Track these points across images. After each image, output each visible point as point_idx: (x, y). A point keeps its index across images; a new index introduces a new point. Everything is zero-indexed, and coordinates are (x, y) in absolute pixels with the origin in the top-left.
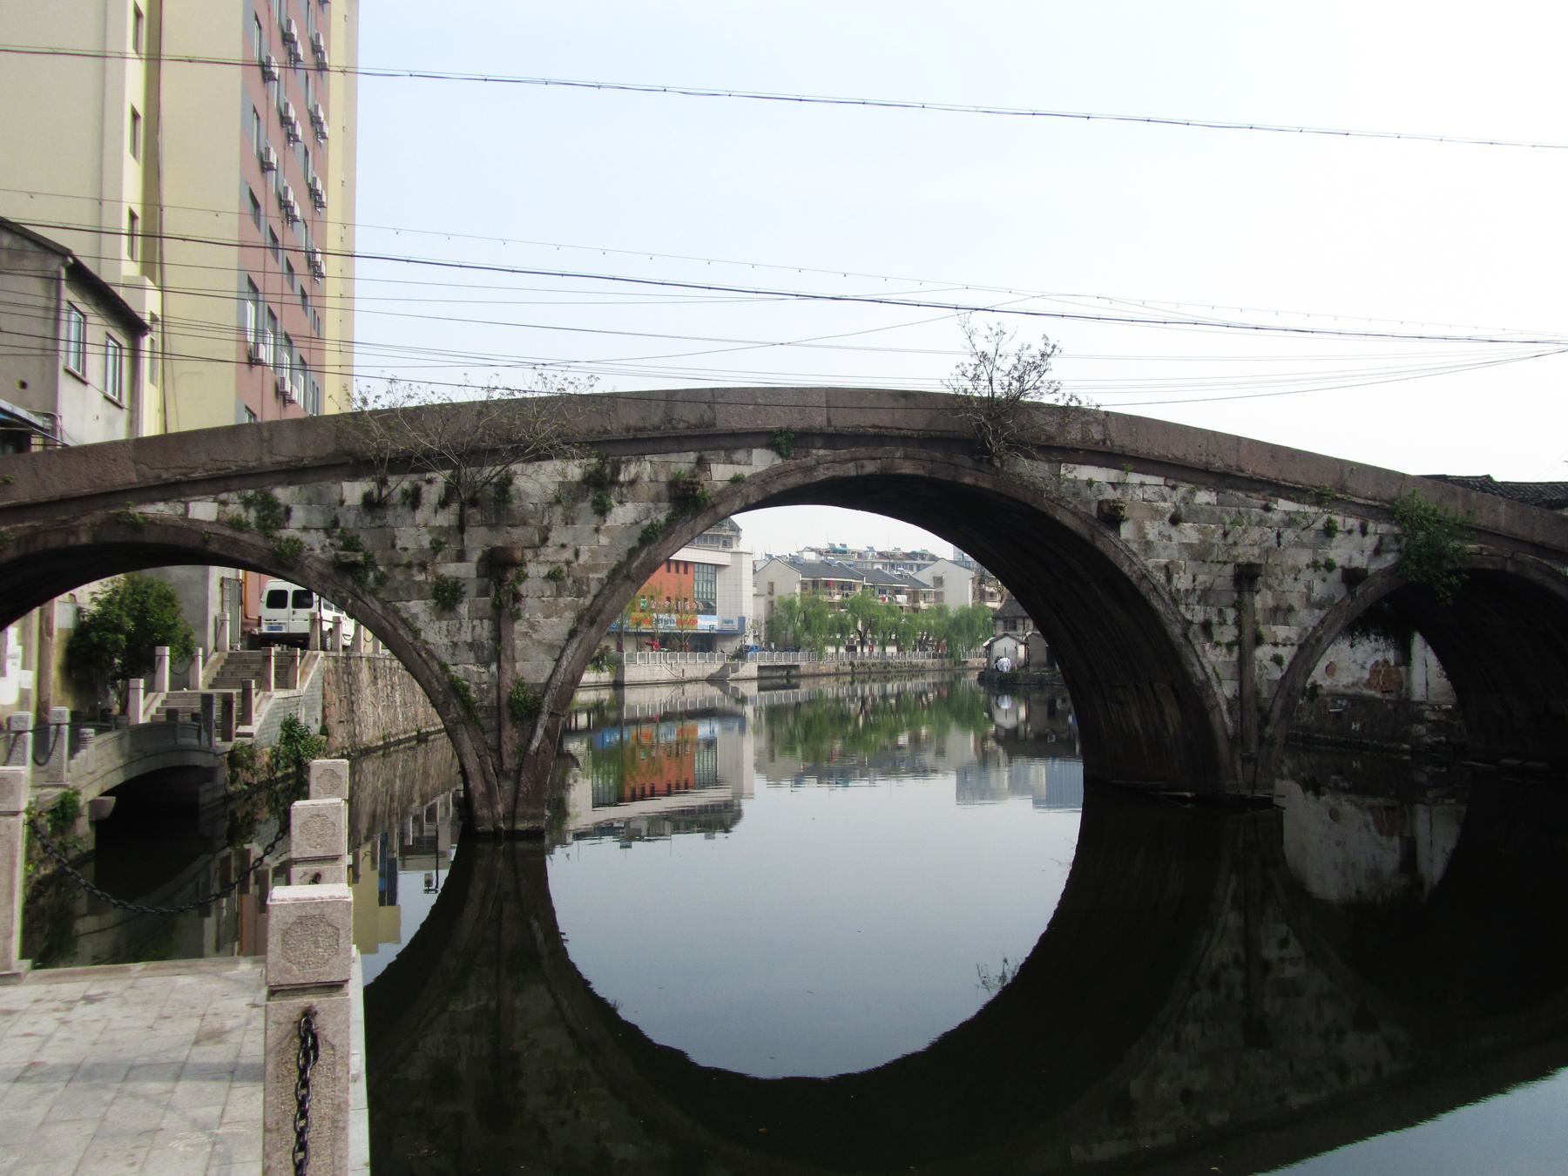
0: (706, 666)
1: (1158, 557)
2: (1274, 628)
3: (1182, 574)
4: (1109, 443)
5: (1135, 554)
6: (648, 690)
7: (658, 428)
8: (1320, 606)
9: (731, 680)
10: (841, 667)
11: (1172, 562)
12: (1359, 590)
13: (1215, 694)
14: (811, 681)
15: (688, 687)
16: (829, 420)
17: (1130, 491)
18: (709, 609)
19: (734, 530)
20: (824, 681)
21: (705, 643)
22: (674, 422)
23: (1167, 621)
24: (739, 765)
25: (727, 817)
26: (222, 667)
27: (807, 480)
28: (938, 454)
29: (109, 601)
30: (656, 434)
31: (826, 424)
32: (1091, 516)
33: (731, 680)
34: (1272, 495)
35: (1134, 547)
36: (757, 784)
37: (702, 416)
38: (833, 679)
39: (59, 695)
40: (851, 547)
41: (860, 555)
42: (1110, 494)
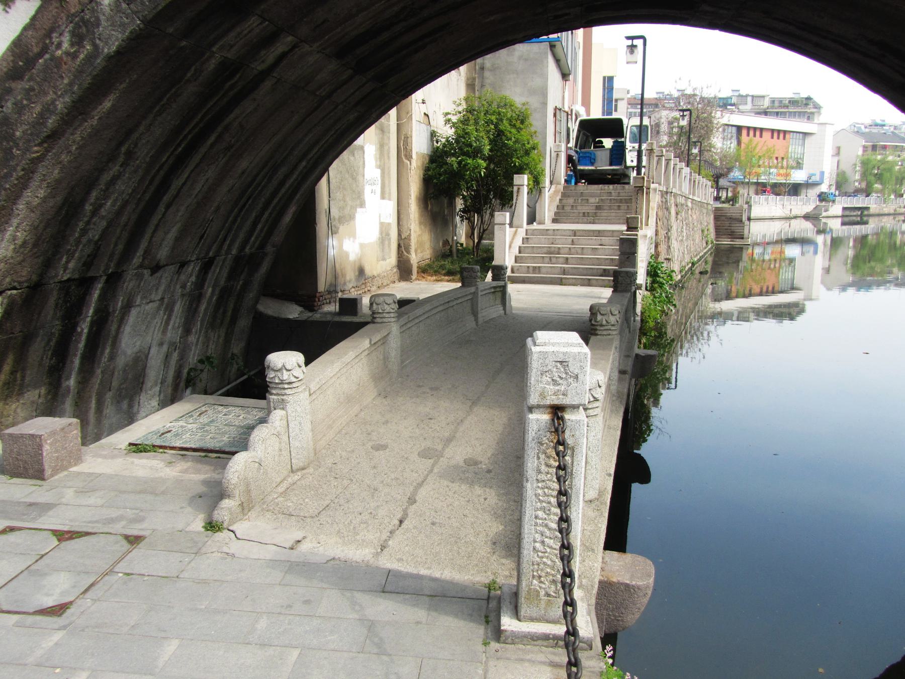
0: (804, 206)
6: (767, 223)
9: (823, 217)
10: (898, 209)
14: (876, 219)
15: (793, 221)
18: (799, 165)
19: (816, 108)
20: (885, 219)
21: (795, 189)
24: (810, 277)
25: (794, 311)
26: (560, 200)
29: (465, 122)
33: (823, 217)
36: (819, 289)
38: (891, 217)
39: (417, 229)
40: (886, 123)
41: (895, 128)
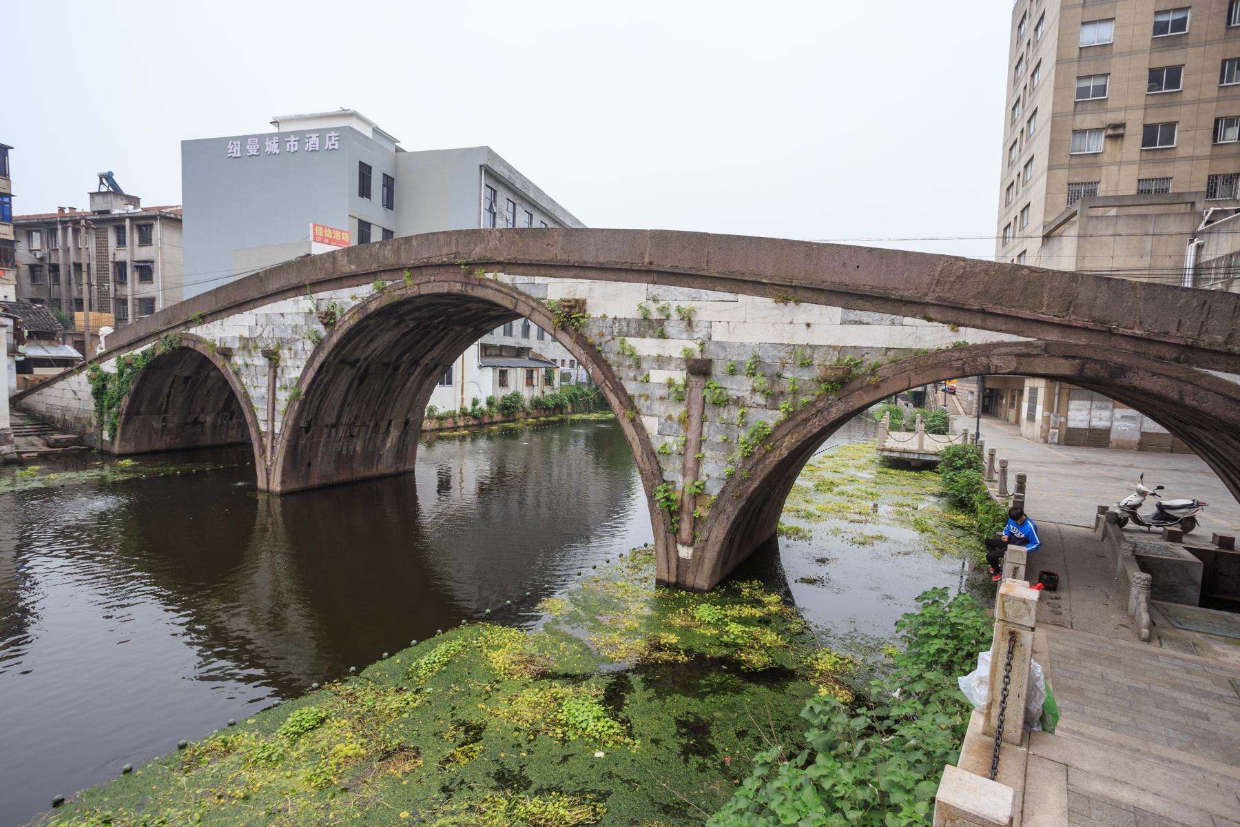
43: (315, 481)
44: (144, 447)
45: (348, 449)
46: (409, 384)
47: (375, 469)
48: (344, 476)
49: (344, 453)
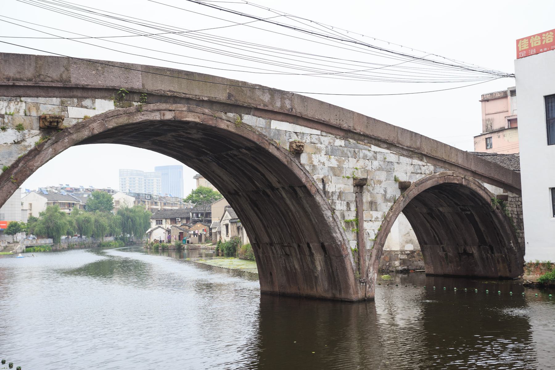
1: (319, 174)
2: (371, 212)
3: (330, 183)
4: (294, 110)
5: (308, 172)
7: (30, 80)
8: (389, 201)
11: (325, 176)
12: (406, 193)
13: (347, 248)
16: (143, 85)
17: (305, 138)
22: (42, 77)
23: (323, 209)
27: (131, 121)
28: (206, 111)
30: (30, 84)
31: (141, 87)
32: (287, 150)
34: (369, 143)
35: (307, 168)
37: (61, 75)
42: (294, 138)
43: (277, 289)
44: (440, 271)
45: (290, 266)
46: (292, 207)
47: (315, 290)
48: (293, 290)
49: (289, 269)
